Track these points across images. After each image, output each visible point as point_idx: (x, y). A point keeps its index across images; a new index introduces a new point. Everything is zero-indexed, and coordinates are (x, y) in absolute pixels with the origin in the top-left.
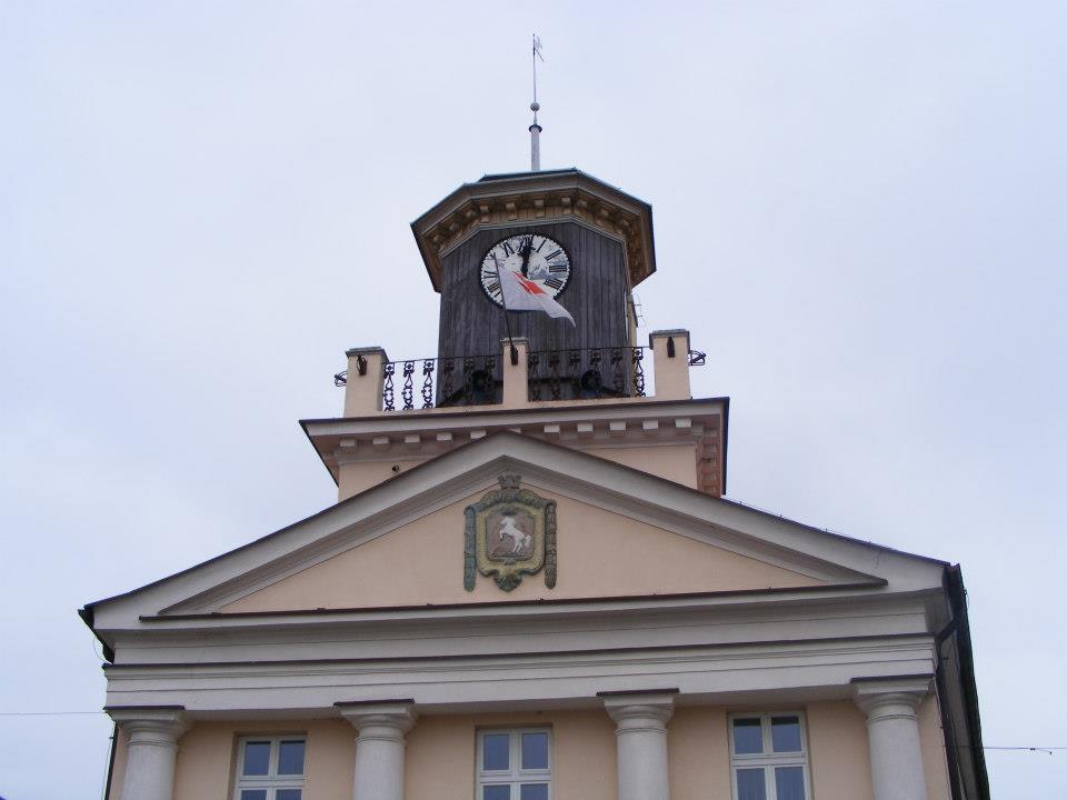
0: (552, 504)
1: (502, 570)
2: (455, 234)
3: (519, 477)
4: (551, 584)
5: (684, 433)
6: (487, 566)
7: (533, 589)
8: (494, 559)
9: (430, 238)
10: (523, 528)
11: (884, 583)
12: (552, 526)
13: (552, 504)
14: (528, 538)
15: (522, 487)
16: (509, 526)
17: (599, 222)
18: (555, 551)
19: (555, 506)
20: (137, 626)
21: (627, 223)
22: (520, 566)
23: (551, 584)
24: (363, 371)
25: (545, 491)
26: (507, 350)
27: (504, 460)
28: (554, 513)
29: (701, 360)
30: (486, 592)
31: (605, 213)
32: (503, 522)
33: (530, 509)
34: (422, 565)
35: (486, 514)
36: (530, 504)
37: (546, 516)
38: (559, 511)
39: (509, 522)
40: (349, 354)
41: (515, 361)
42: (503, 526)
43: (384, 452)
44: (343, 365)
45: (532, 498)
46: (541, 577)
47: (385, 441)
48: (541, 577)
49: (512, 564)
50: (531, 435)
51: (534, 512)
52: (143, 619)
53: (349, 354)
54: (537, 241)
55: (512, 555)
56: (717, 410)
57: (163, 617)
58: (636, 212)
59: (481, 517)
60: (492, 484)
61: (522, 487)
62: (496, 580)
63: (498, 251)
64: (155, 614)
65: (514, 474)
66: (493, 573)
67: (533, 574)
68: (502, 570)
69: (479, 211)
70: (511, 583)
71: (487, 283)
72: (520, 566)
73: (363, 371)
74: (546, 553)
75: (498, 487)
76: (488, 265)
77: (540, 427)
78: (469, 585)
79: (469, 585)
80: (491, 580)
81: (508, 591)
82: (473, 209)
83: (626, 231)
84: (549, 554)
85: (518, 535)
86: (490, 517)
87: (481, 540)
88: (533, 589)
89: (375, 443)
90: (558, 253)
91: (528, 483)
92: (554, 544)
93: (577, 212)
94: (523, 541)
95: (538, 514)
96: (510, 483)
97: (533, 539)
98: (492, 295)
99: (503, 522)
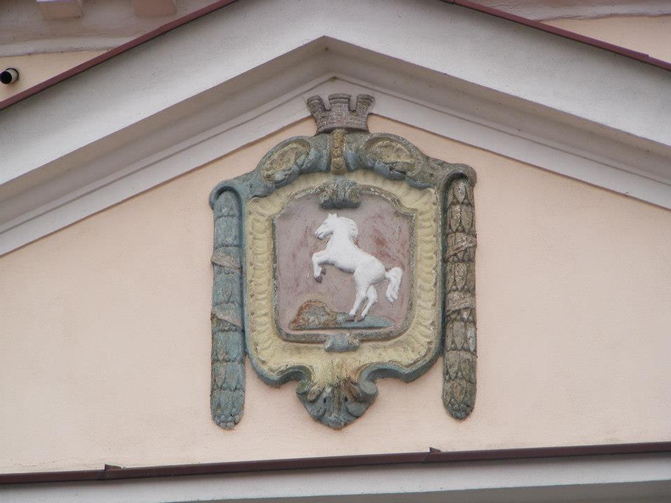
0: (463, 176)
3: (368, 100)
6: (277, 357)
7: (409, 420)
8: (297, 334)
10: (380, 248)
12: (461, 241)
13: (463, 176)
14: (395, 275)
15: (376, 128)
16: (341, 239)
18: (472, 311)
19: (472, 184)
22: (371, 355)
25: (441, 139)
27: (325, 49)
28: (469, 203)
33: (398, 190)
35: (272, 207)
36: (398, 176)
37: (445, 210)
38: (482, 195)
39: (339, 227)
42: (323, 241)
45: (404, 159)
46: (434, 385)
48: (434, 385)
49: (350, 349)
51: (411, 200)
55: (351, 323)
59: (260, 214)
60: (289, 119)
61: (376, 128)
62: (303, 396)
65: (355, 92)
66: (294, 376)
67: (411, 377)
70: (346, 403)
72: (371, 355)
74: (446, 319)
75: (308, 130)
78: (226, 413)
79: (226, 413)
80: (288, 396)
81: (338, 426)
84: (455, 319)
85: (366, 266)
86: (286, 216)
87: (259, 279)
88: (409, 420)
91: (392, 116)
92: (470, 290)
94: (380, 283)
95: (424, 204)
96: (340, 117)
97: (409, 284)
99: (321, 231)
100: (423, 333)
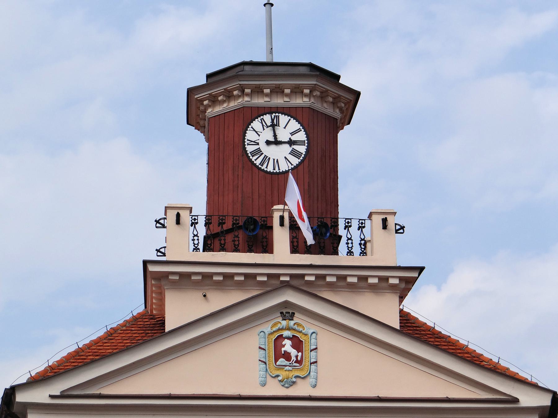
2: (221, 104)
5: (393, 286)
9: (201, 101)
11: (516, 401)
14: (300, 354)
17: (325, 105)
21: (343, 105)
26: (276, 216)
29: (401, 231)
30: (274, 389)
31: (331, 99)
32: (284, 343)
41: (282, 224)
42: (284, 346)
43: (196, 285)
47: (200, 278)
50: (297, 283)
52: (52, 397)
54: (283, 119)
56: (415, 274)
57: (63, 395)
58: (351, 97)
63: (256, 124)
64: (59, 394)
69: (243, 91)
71: (250, 149)
76: (250, 135)
77: (303, 276)
80: (276, 381)
82: (239, 90)
83: (341, 109)
89: (192, 278)
90: (298, 131)
93: (312, 100)
98: (253, 159)
99: (284, 343)
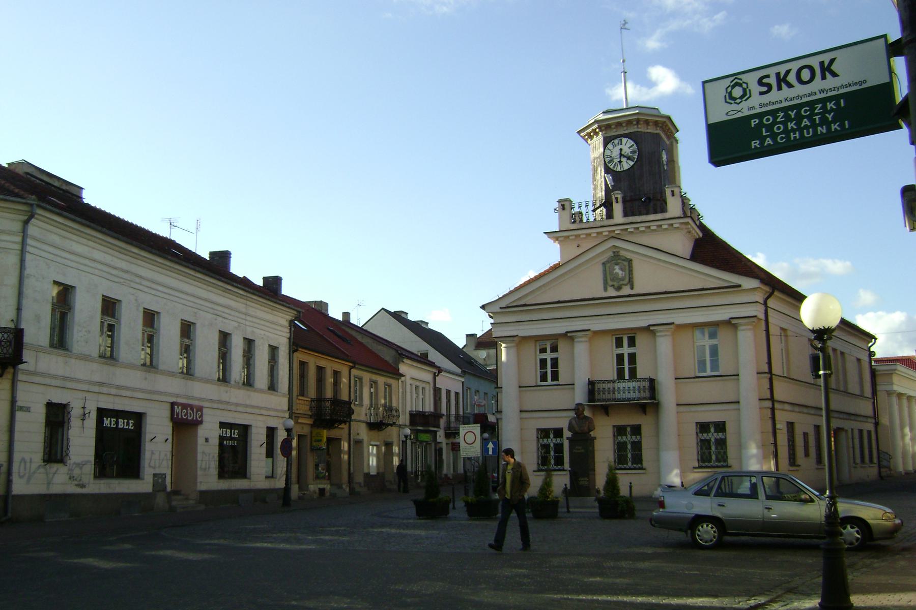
0: (631, 260)
1: (616, 284)
4: (632, 288)
7: (626, 291)
8: (612, 280)
10: (621, 269)
13: (631, 260)
20: (499, 310)
23: (632, 288)
24: (564, 209)
25: (629, 256)
30: (612, 292)
34: (591, 284)
39: (617, 267)
40: (559, 201)
44: (557, 205)
53: (559, 201)
59: (608, 265)
60: (610, 254)
68: (616, 284)
70: (619, 288)
73: (564, 209)
78: (605, 289)
79: (605, 289)
85: (620, 272)
91: (622, 253)
95: (626, 263)
100: (627, 280)
